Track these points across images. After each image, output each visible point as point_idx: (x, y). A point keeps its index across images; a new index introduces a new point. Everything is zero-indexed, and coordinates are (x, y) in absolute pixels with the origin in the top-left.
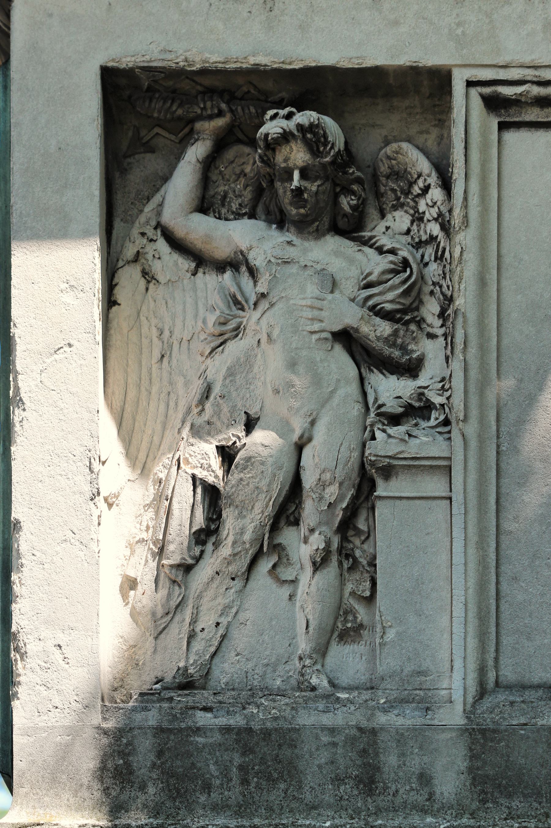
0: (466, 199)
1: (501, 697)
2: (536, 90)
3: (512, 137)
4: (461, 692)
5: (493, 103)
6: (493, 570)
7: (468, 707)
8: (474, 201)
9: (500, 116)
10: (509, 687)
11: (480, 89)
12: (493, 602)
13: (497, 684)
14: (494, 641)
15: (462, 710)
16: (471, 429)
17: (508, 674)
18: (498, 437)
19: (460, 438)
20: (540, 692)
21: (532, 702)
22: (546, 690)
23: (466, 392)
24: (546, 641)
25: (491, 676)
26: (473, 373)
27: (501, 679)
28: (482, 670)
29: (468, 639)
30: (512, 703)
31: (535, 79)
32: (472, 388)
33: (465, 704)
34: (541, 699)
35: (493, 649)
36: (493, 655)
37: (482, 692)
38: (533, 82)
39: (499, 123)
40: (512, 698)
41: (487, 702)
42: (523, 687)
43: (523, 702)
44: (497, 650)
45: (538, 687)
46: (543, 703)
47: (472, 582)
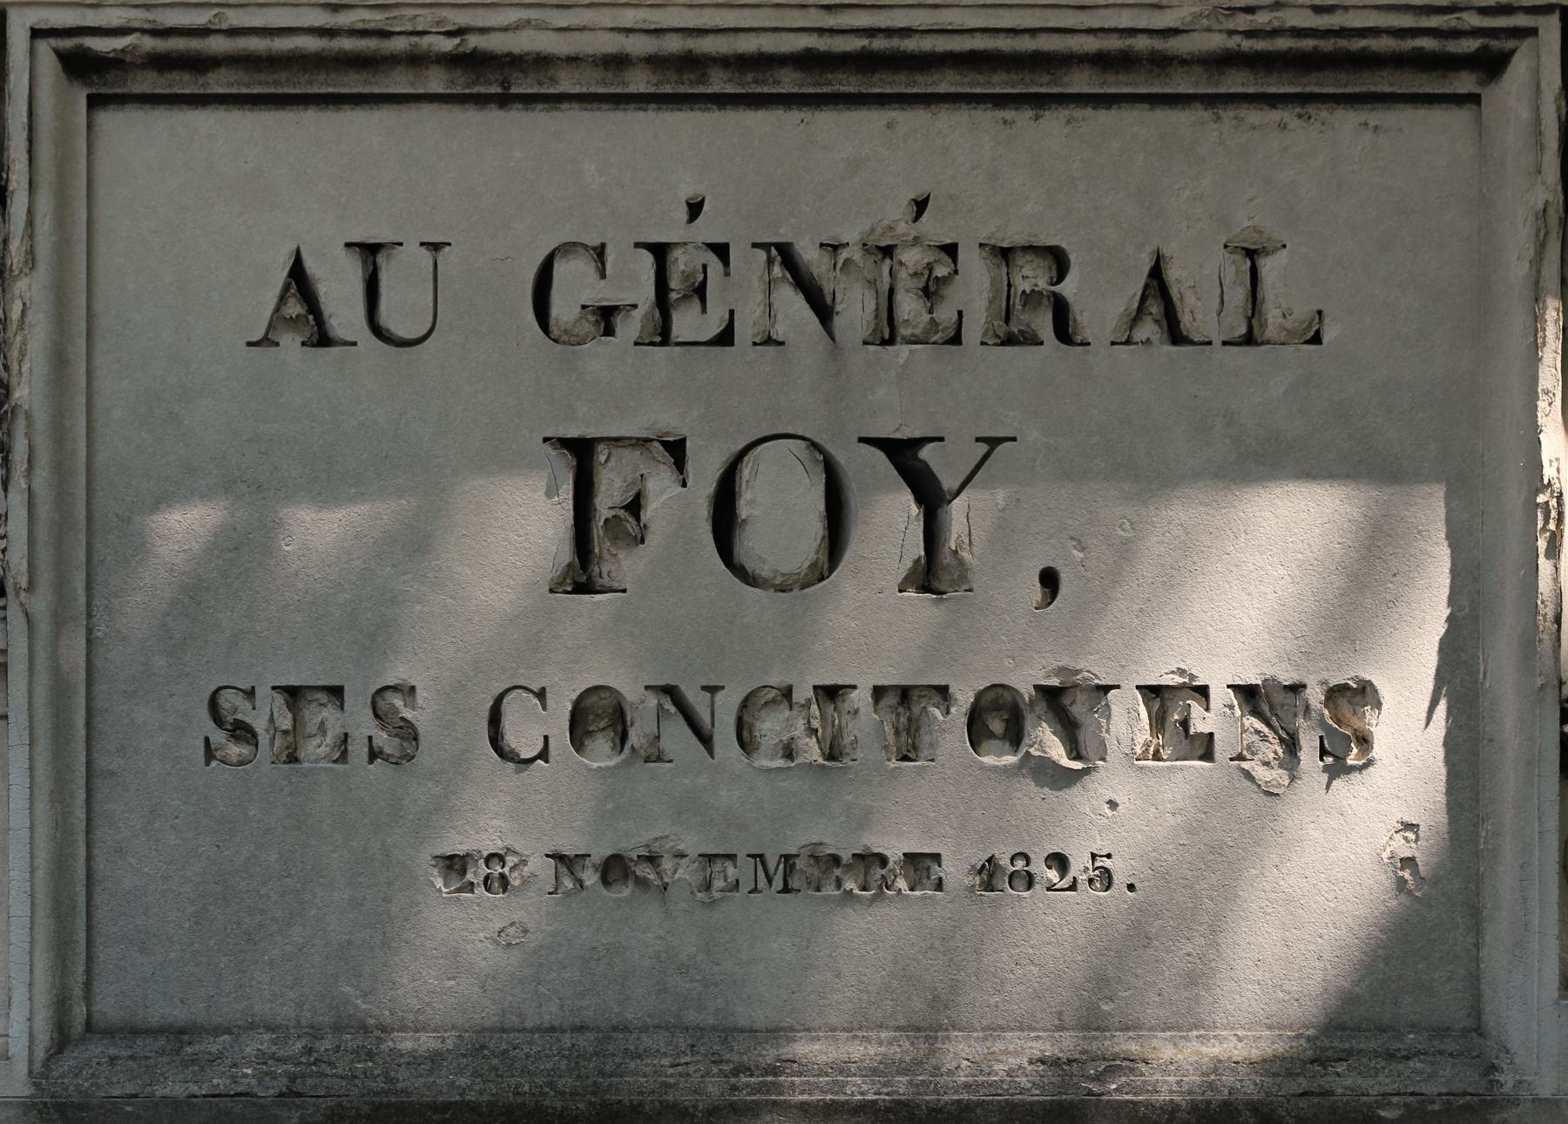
0: (30, 222)
1: (97, 1050)
2: (149, 44)
3: (109, 119)
4: (25, 1041)
5: (78, 65)
6: (81, 837)
7: (38, 1067)
8: (44, 226)
9: (90, 85)
10: (109, 1032)
11: (54, 42)
12: (81, 890)
13: (89, 1026)
14: (83, 956)
15: (25, 1070)
16: (41, 604)
17: (108, 1006)
18: (89, 615)
19: (23, 619)
20: (162, 1041)
21: (147, 1058)
22: (172, 1037)
23: (31, 542)
24: (172, 955)
25: (79, 1012)
26: (44, 510)
27: (96, 1017)
28: (61, 1005)
29: (37, 954)
30: (113, 1060)
31: (147, 26)
32: (43, 535)
33: (31, 1062)
34: (163, 1052)
35: (81, 968)
36: (81, 978)
37: (62, 1040)
38: (144, 31)
39: (89, 97)
40: (112, 1051)
41: (70, 1060)
42: (134, 1031)
43: (131, 1057)
44: (89, 971)
45: (160, 1031)
46: (165, 1059)
47: (42, 859)
